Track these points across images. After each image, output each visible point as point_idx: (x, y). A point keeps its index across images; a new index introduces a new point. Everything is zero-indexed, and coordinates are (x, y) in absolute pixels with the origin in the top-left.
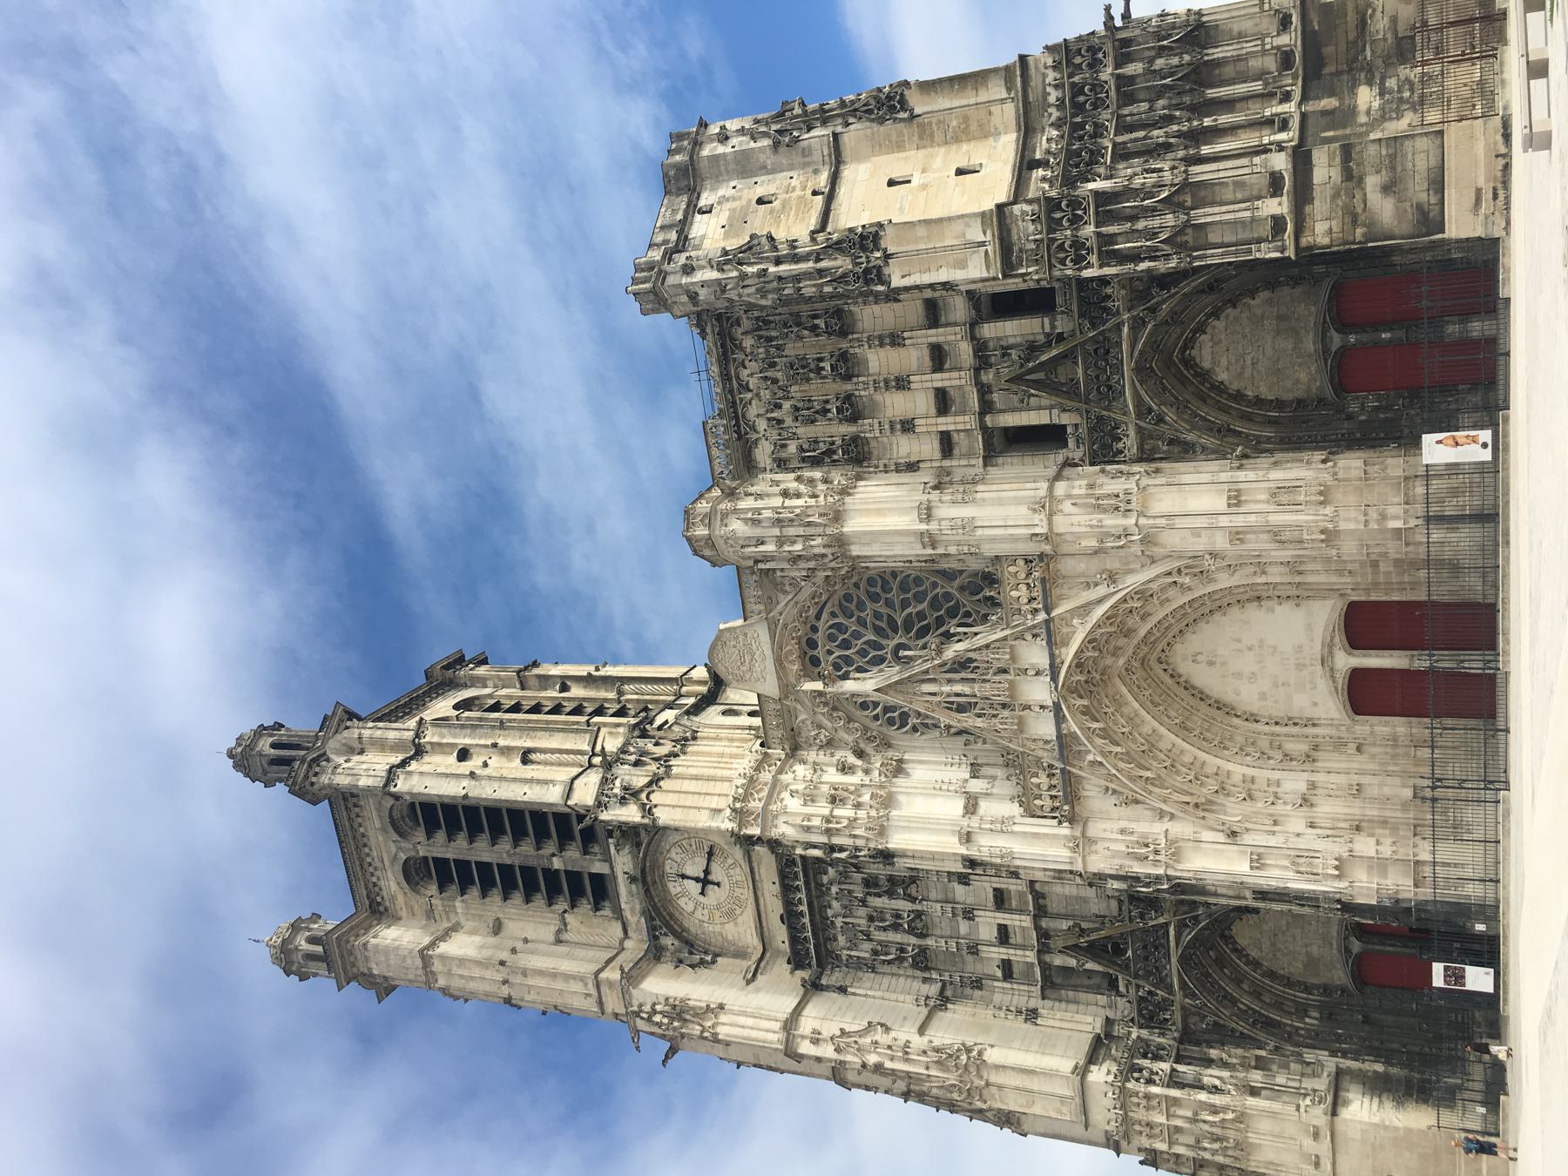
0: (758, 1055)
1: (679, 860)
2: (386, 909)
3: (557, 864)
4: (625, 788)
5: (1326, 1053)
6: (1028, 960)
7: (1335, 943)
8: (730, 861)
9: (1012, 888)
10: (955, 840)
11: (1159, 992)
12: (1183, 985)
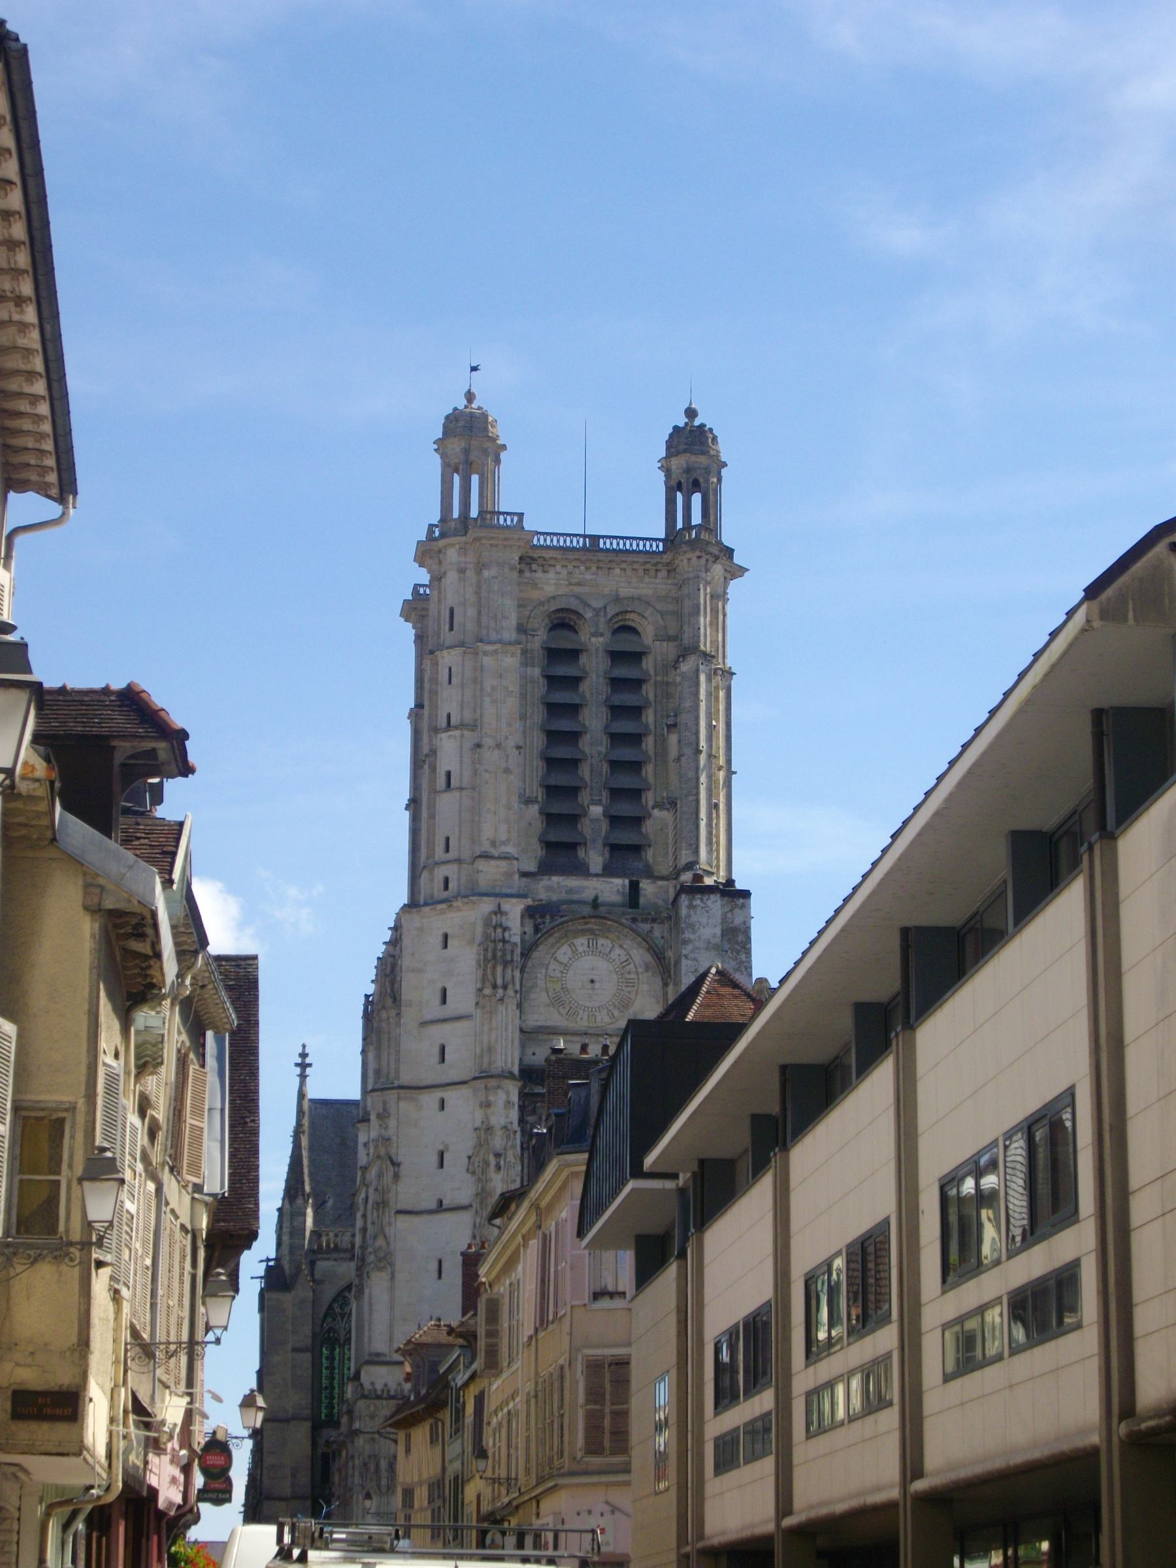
3: (596, 811)
8: (616, 1013)
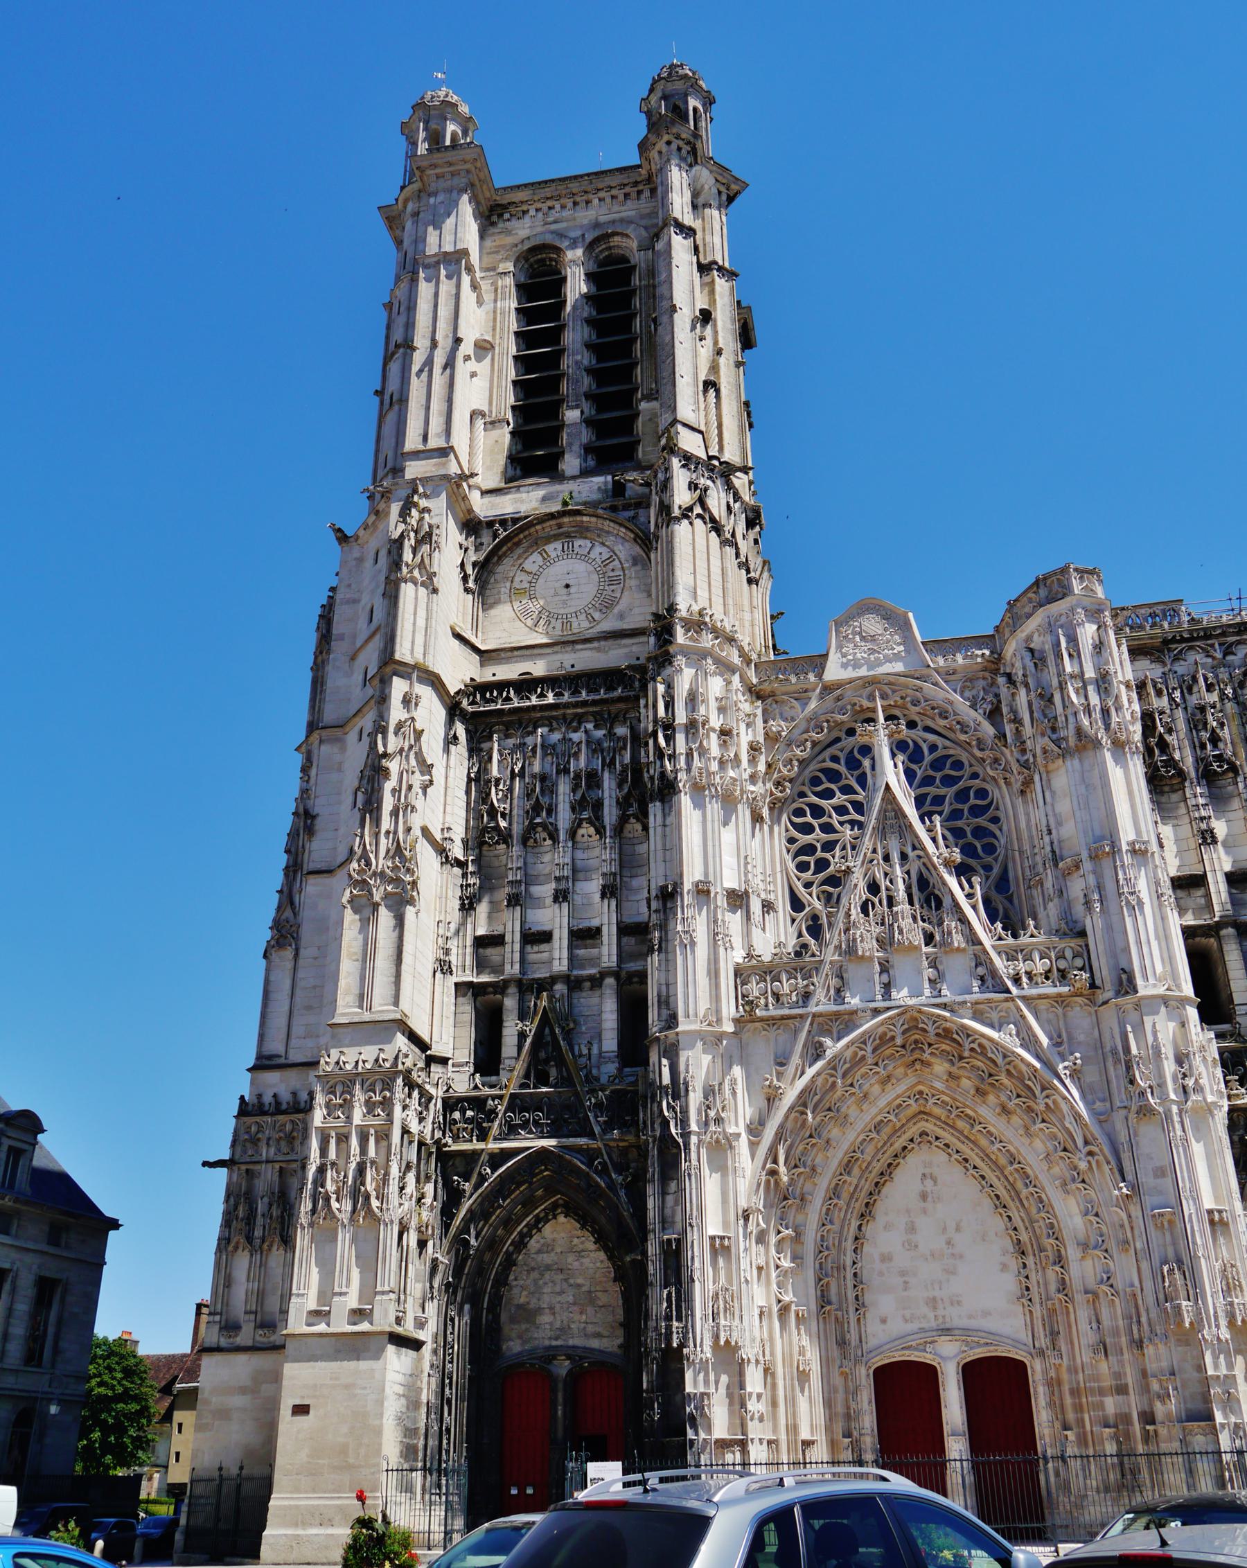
0: (342, 639)
1: (592, 555)
2: (493, 224)
3: (572, 415)
4: (706, 490)
5: (435, 1330)
6: (508, 967)
7: (559, 1343)
8: (597, 615)
9: (605, 950)
10: (698, 876)
11: (497, 1123)
12: (506, 1155)
